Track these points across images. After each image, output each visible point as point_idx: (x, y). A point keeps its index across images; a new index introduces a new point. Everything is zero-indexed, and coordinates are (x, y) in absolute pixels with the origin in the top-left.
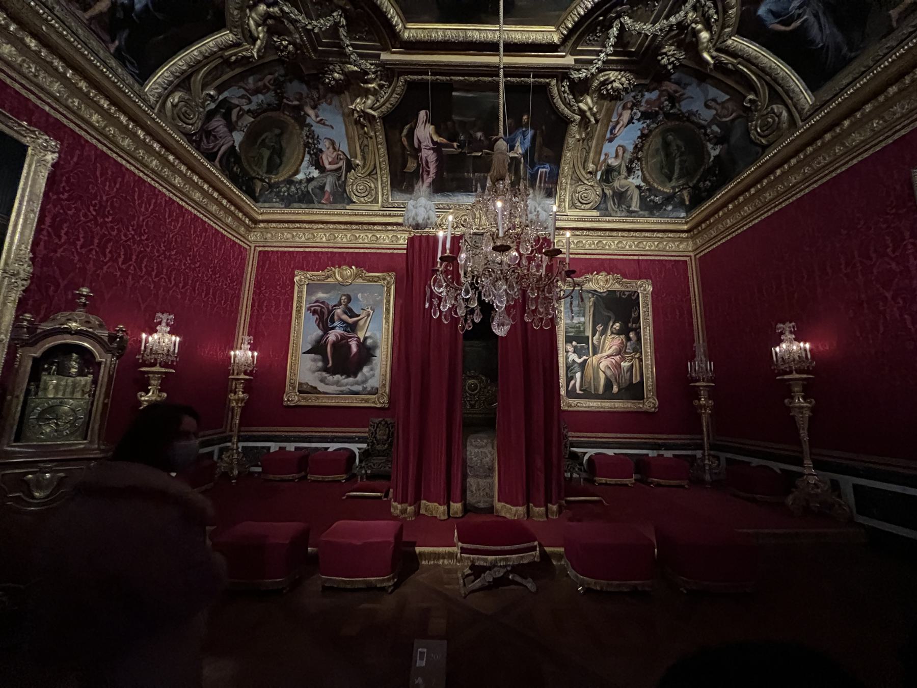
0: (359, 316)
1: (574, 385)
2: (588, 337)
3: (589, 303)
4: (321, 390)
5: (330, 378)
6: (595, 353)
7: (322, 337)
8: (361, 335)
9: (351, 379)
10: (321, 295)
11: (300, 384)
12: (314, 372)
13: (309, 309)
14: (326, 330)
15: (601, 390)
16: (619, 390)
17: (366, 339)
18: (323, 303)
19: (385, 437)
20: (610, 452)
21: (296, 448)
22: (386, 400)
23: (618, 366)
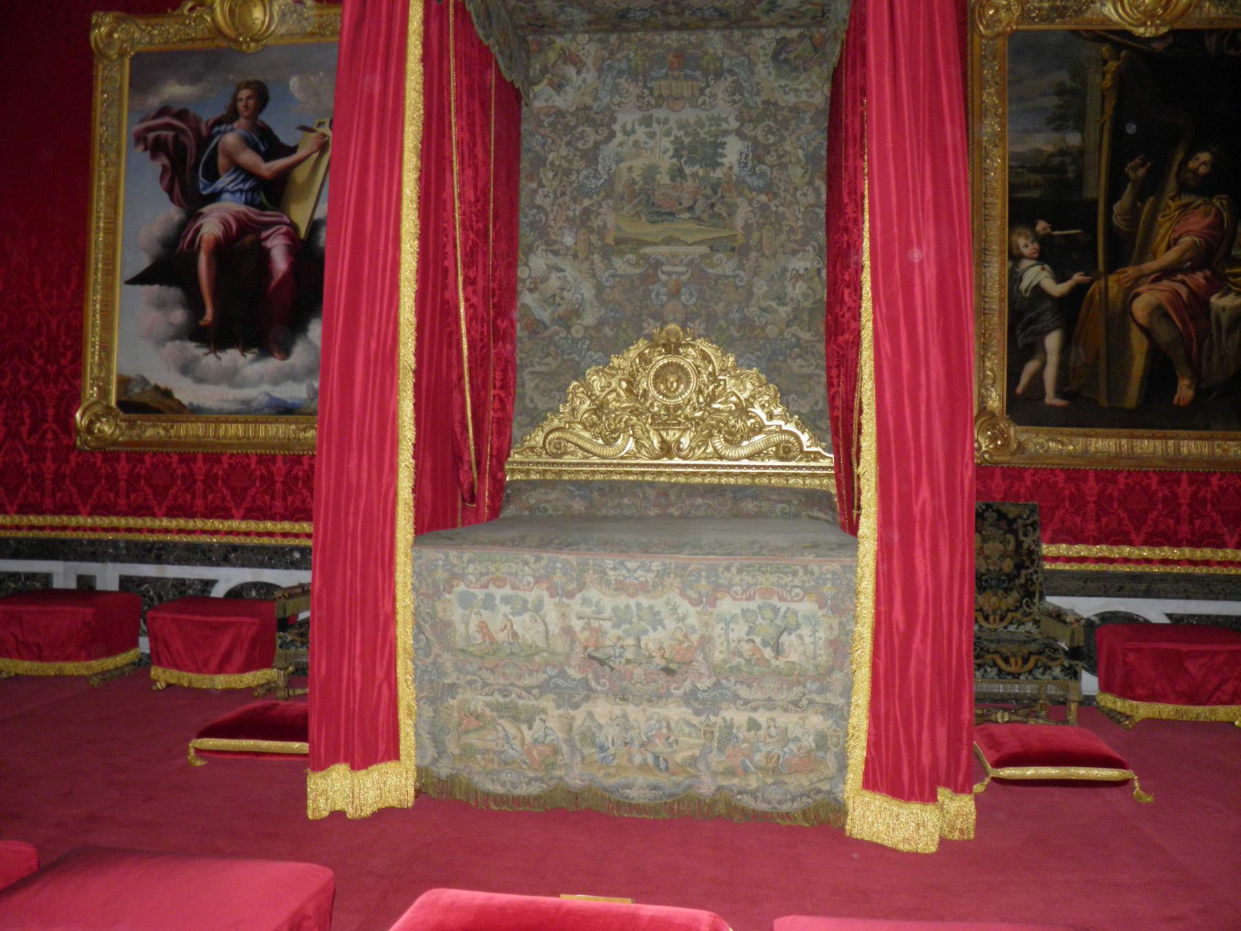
0: (293, 150)
1: (1038, 377)
2: (1095, 203)
3: (1102, 80)
4: (185, 401)
5: (210, 361)
6: (1115, 263)
7: (183, 227)
8: (301, 215)
9: (273, 364)
10: (175, 91)
11: (124, 382)
12: (161, 342)
13: (140, 138)
14: (194, 204)
15: (1132, 397)
16: (1199, 393)
17: (315, 226)
18: (182, 115)
20: (1154, 611)
21: (125, 581)
23: (1198, 305)
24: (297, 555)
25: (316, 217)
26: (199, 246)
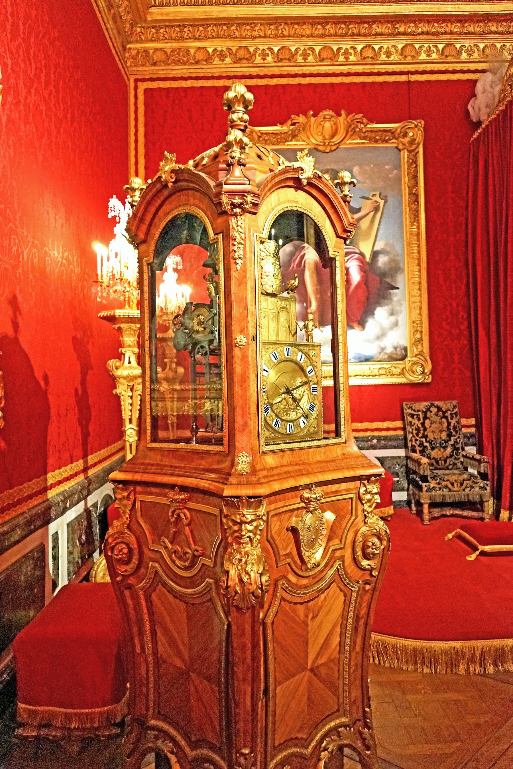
0: (359, 210)
17: (375, 254)
19: (444, 436)
22: (428, 368)
24: (375, 441)
25: (375, 249)
26: (304, 266)
